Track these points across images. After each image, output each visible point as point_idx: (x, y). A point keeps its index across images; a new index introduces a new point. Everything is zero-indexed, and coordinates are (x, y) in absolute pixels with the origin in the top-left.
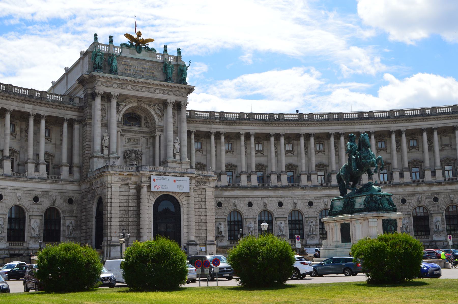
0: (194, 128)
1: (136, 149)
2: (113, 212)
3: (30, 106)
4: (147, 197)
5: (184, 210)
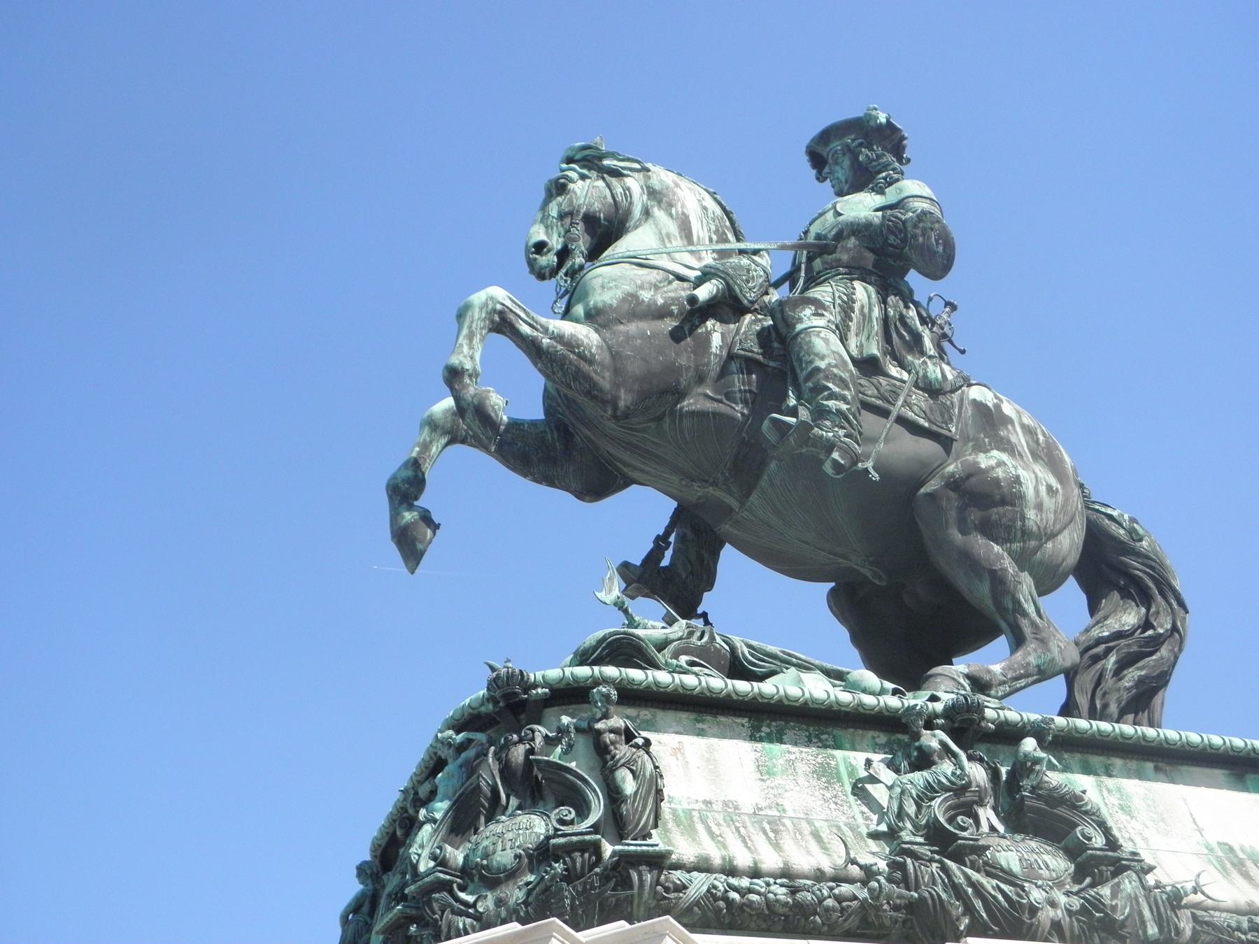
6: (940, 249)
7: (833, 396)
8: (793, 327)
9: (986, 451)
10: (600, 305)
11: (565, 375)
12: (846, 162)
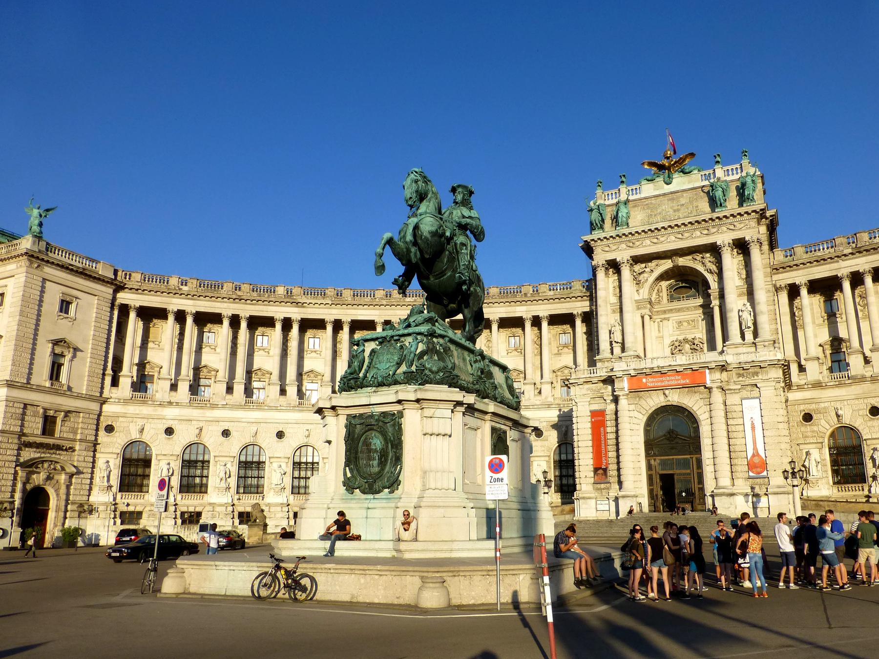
0: (801, 277)
1: (690, 337)
2: (580, 444)
3: (524, 308)
4: (627, 413)
5: (705, 430)
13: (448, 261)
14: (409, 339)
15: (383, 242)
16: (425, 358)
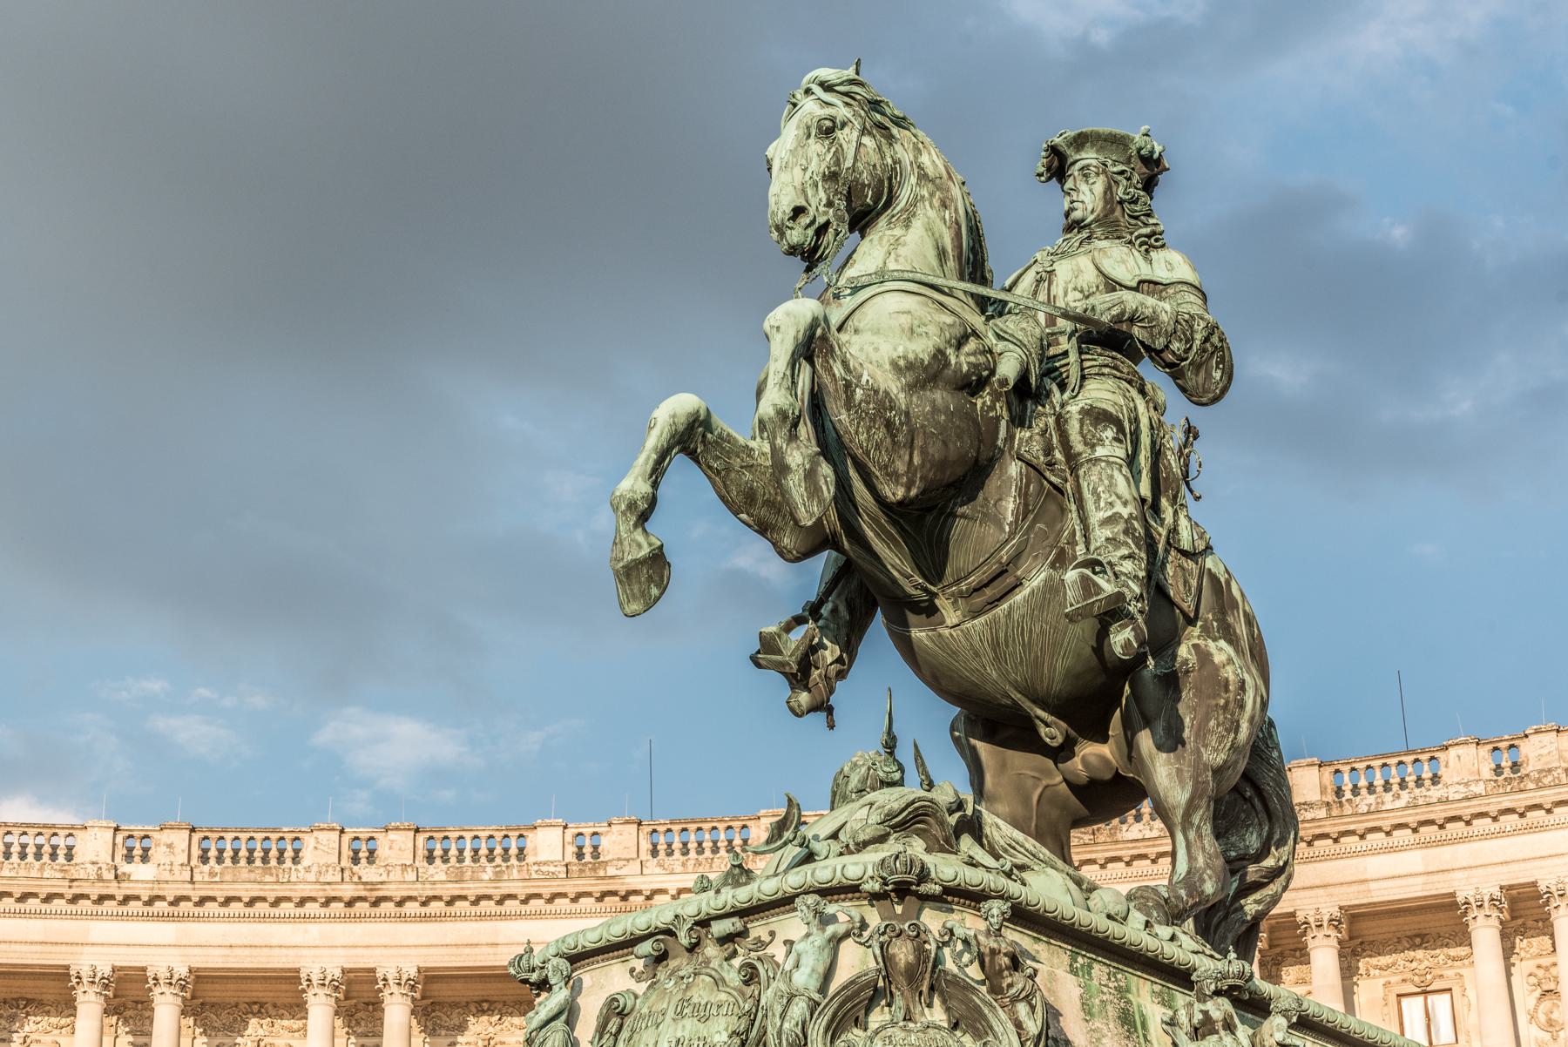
6: (1217, 375)
7: (1130, 556)
8: (1093, 446)
9: (1215, 640)
10: (911, 356)
11: (868, 440)
12: (1099, 185)
13: (1024, 512)
14: (791, 926)
15: (654, 439)
16: (877, 1018)
